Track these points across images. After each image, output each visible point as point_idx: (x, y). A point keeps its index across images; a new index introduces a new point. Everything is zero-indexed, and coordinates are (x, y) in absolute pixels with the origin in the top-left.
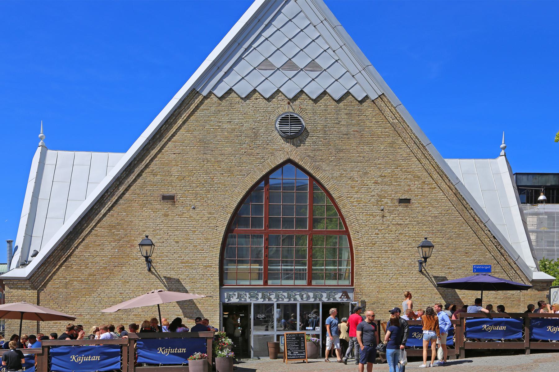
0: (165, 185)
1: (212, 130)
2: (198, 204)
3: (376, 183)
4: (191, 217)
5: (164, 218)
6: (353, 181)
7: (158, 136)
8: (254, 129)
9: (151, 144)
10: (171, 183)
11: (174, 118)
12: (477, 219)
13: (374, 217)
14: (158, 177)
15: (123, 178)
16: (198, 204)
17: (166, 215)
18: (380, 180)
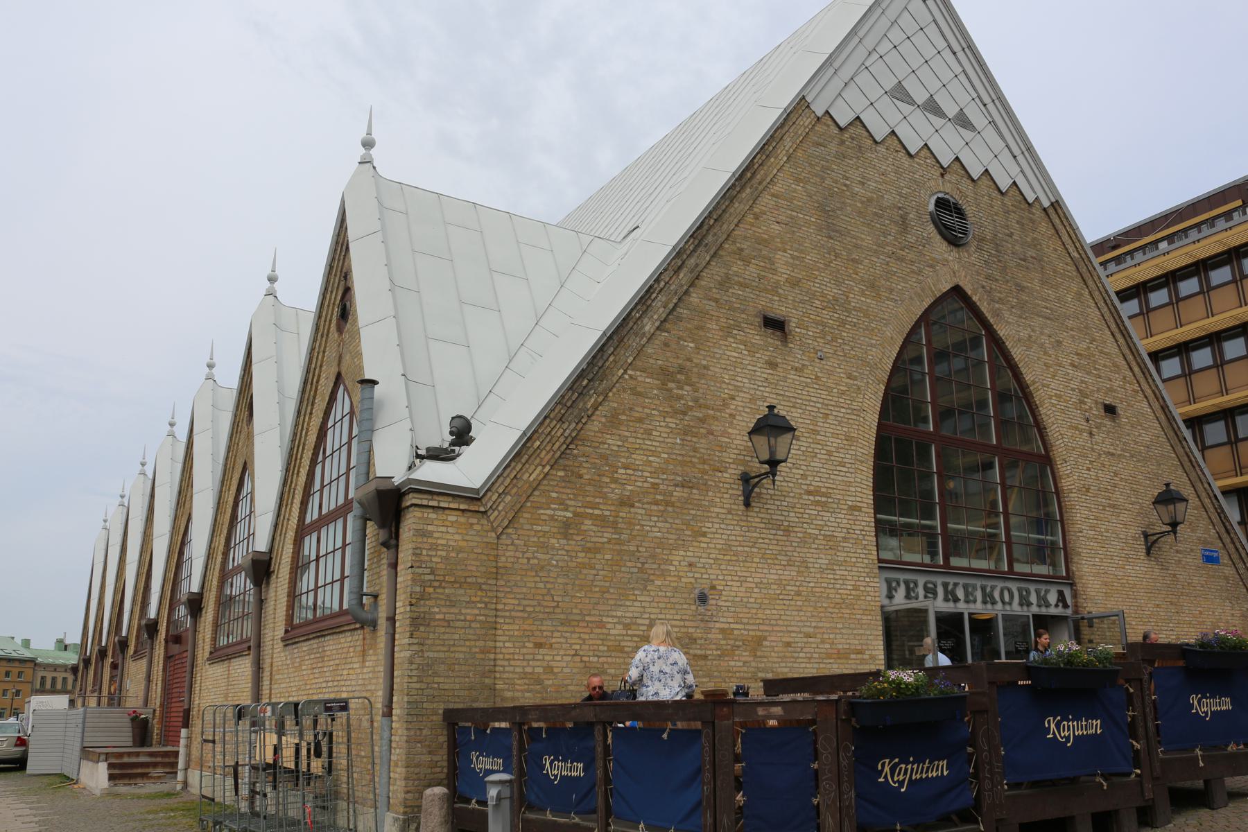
0: (766, 290)
1: (836, 189)
2: (828, 349)
3: (1072, 365)
4: (817, 378)
5: (768, 371)
6: (1045, 353)
7: (749, 175)
8: (900, 208)
9: (738, 189)
10: (774, 290)
11: (774, 144)
12: (1193, 459)
13: (1081, 431)
14: (752, 268)
15: (688, 252)
16: (828, 349)
17: (773, 365)
18: (1075, 358)
